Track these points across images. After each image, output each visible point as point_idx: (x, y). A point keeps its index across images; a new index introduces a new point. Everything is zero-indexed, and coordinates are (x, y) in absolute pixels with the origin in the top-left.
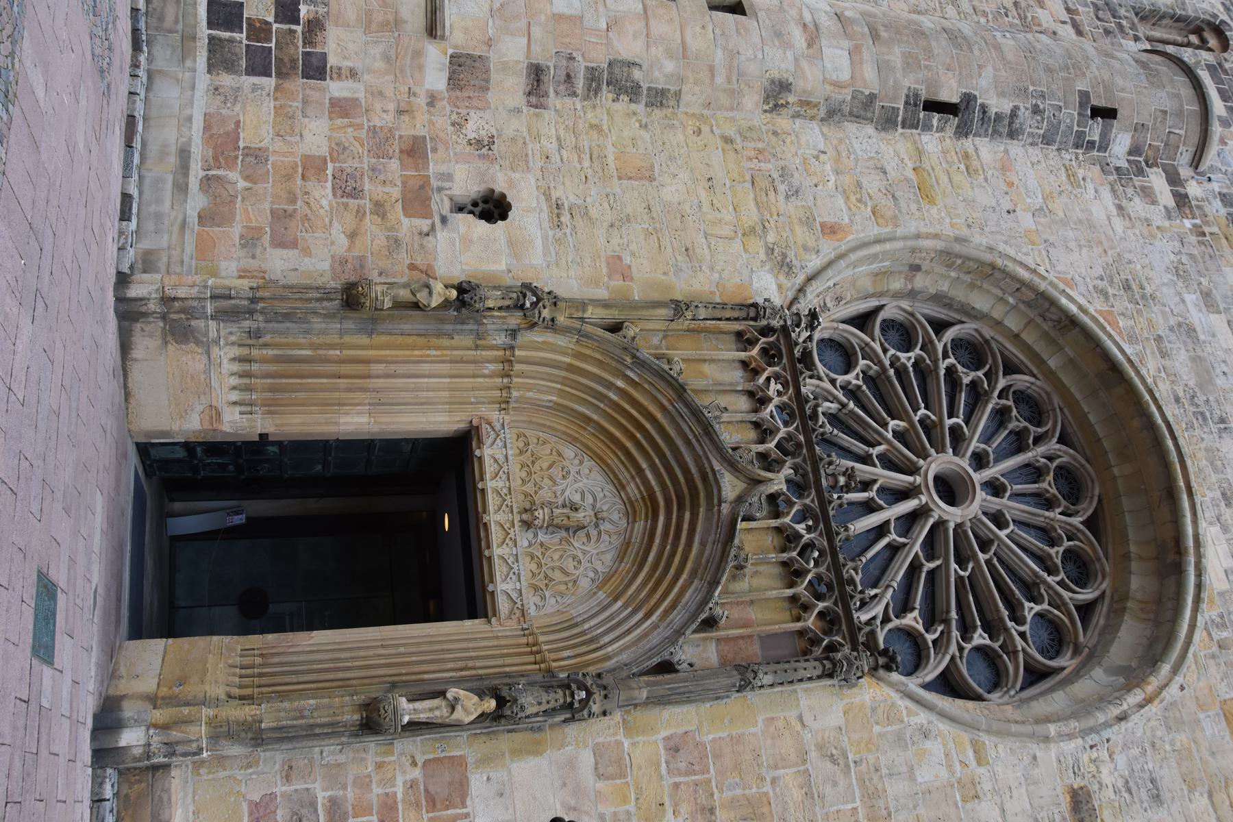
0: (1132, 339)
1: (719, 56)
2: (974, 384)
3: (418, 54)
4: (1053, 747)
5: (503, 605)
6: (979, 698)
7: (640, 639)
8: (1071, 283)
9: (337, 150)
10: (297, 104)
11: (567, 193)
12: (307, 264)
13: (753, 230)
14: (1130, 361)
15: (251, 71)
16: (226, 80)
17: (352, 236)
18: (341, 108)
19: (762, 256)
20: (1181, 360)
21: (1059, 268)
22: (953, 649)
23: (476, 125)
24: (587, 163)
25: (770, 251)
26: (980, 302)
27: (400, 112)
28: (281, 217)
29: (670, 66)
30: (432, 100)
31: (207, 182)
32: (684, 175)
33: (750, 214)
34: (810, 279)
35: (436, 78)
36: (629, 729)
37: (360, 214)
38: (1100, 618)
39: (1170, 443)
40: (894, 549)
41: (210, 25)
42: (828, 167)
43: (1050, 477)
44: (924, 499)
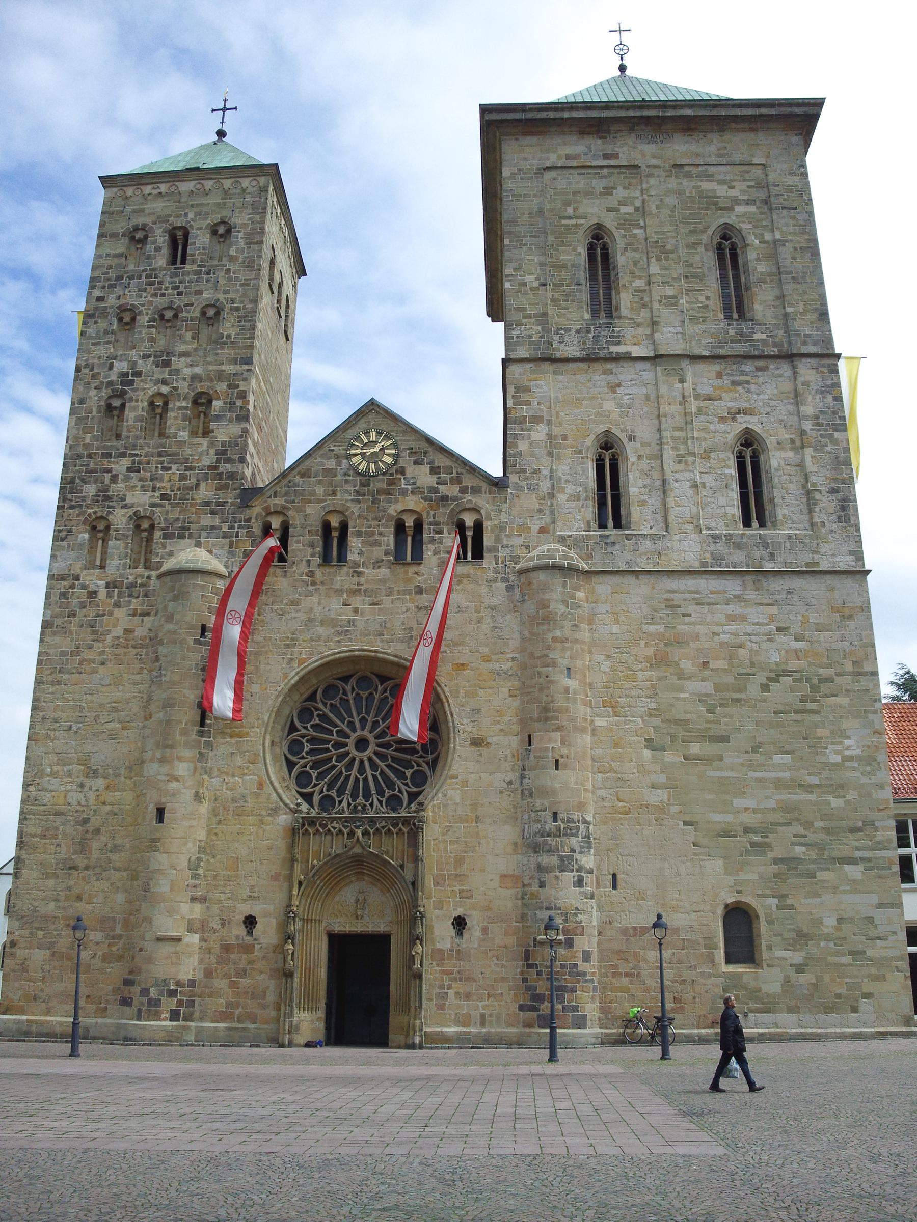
0: (312, 654)
1: (185, 823)
2: (319, 715)
3: (187, 945)
4: (458, 748)
5: (387, 929)
6: (439, 754)
8: (285, 676)
9: (226, 976)
10: (207, 990)
11: (246, 892)
12: (272, 988)
14: (322, 658)
15: (193, 1006)
16: (197, 1015)
17: (261, 972)
18: (208, 974)
19: (270, 818)
23: (215, 924)
24: (231, 883)
25: (269, 815)
26: (286, 711)
27: (210, 952)
29: (190, 845)
30: (202, 940)
31: (239, 1021)
32: (236, 845)
34: (281, 800)
35: (195, 938)
36: (429, 898)
37: (253, 969)
39: (357, 653)
40: (382, 773)
41: (178, 1021)
43: (361, 693)
44: (365, 758)
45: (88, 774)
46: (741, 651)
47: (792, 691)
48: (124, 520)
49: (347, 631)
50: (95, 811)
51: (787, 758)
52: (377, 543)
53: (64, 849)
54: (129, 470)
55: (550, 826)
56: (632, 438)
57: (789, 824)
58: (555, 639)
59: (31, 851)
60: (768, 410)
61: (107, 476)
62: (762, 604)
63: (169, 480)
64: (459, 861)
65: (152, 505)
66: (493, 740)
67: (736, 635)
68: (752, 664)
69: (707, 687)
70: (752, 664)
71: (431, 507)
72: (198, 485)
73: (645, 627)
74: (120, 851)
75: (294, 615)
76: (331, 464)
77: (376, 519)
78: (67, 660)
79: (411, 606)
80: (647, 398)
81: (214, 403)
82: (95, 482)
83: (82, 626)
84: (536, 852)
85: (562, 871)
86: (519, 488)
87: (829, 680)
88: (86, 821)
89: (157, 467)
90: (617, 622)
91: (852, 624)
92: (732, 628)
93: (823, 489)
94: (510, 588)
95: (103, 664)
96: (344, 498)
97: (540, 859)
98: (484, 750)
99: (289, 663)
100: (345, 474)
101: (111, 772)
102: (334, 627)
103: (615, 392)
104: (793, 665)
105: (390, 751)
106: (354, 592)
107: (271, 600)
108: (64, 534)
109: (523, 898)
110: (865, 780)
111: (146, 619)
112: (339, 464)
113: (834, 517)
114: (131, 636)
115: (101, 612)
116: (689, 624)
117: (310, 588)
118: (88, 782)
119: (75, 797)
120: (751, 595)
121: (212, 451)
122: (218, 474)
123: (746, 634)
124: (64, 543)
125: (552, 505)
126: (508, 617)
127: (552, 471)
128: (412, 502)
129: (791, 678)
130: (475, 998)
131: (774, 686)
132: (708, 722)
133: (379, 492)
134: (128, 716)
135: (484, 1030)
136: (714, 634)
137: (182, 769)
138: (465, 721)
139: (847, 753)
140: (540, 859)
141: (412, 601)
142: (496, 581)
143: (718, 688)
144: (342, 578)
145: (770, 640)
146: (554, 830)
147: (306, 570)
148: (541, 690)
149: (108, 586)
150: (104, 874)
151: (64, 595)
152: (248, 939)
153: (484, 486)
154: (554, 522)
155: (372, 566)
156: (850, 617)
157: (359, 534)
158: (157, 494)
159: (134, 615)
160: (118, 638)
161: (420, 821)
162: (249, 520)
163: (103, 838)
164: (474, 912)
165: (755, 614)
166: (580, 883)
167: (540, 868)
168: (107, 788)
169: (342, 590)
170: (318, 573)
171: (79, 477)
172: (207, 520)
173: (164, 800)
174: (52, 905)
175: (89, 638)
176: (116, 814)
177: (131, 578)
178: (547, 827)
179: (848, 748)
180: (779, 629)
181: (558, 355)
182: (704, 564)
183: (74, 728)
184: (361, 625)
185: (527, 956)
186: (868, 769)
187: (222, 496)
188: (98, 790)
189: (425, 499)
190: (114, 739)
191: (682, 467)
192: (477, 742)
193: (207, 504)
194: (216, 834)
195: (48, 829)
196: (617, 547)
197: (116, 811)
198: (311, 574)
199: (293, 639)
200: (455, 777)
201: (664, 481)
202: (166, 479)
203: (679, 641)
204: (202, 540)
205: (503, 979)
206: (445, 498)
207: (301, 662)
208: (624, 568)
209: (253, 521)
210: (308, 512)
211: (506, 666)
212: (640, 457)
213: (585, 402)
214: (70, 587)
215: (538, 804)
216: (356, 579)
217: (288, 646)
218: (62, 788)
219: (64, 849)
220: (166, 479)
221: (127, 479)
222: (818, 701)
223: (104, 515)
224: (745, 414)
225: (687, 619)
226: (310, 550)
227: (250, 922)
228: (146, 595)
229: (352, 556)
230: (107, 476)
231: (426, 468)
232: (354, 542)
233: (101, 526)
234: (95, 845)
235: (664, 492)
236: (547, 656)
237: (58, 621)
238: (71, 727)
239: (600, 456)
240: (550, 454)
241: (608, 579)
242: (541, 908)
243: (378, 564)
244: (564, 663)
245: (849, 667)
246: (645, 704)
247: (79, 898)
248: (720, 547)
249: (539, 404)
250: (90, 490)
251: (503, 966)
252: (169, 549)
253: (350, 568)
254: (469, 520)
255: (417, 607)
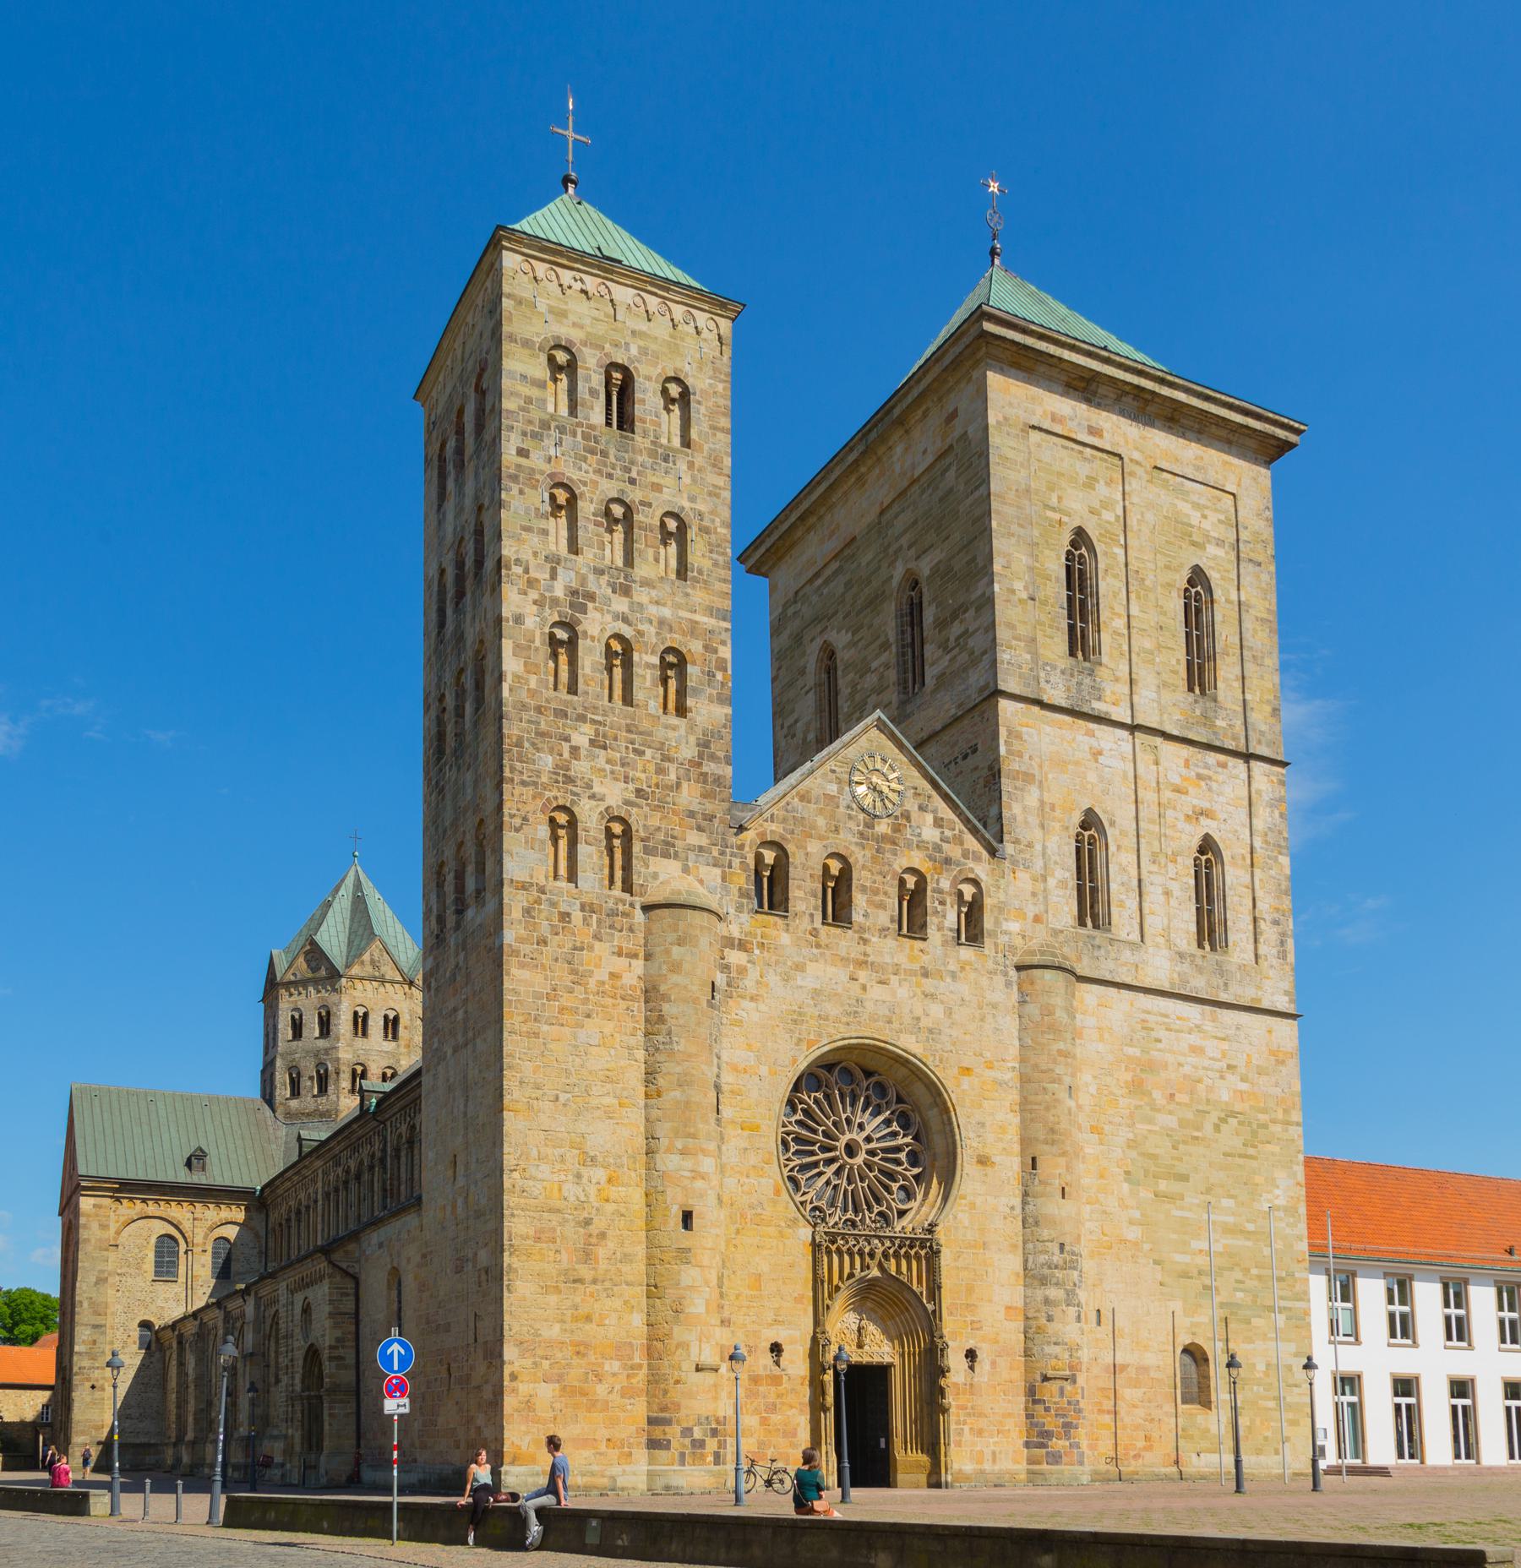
0: (820, 1035)
5: (891, 1360)
7: (918, 1318)
8: (794, 1061)
9: (756, 1411)
11: (770, 1316)
13: (780, 1232)
17: (791, 1407)
20: (833, 1010)
21: (787, 1063)
22: (908, 1173)
28: (785, 1434)
33: (771, 1230)
37: (783, 1404)
38: (903, 1093)
39: (867, 1041)
42: (747, 1181)
45: (585, 1161)
46: (1201, 1087)
47: (1237, 1134)
48: (595, 816)
49: (856, 1012)
50: (597, 1209)
51: (1230, 1203)
52: (881, 906)
53: (564, 1256)
54: (592, 742)
55: (1057, 1258)
56: (1112, 824)
57: (1231, 1269)
58: (1060, 1052)
59: (525, 1258)
60: (1225, 816)
61: (566, 746)
62: (1216, 1038)
63: (643, 773)
64: (970, 1290)
65: (627, 803)
66: (996, 1159)
67: (1194, 1067)
68: (1208, 1100)
69: (1171, 1121)
70: (1208, 1100)
71: (935, 869)
72: (678, 785)
73: (1125, 1048)
74: (631, 1261)
75: (799, 983)
76: (833, 789)
77: (880, 873)
78: (544, 1004)
79: (919, 991)
80: (1125, 773)
81: (690, 669)
82: (551, 751)
83: (556, 960)
84: (1043, 1284)
85: (1068, 1305)
86: (1015, 863)
87: (1265, 1126)
88: (587, 1222)
89: (627, 748)
90: (1102, 1039)
91: (1284, 1069)
92: (1192, 1059)
93: (1266, 916)
94: (1008, 984)
95: (588, 1016)
96: (847, 841)
97: (1048, 1292)
98: (989, 1170)
99: (797, 1044)
100: (848, 807)
101: (612, 1161)
102: (842, 1005)
103: (1096, 761)
104: (1238, 1107)
105: (876, 1159)
106: (861, 964)
107: (774, 958)
108: (517, 822)
109: (1025, 1332)
110: (1288, 1231)
111: (634, 962)
112: (840, 791)
113: (1274, 951)
114: (619, 984)
115: (578, 944)
116: (1159, 1050)
117: (815, 951)
118: (584, 1171)
119: (571, 1190)
120: (1208, 1026)
121: (692, 739)
122: (702, 774)
123: (1204, 1068)
124: (521, 836)
125: (1045, 890)
126: (1008, 1018)
127: (1044, 848)
128: (917, 860)
129: (1235, 1120)
130: (986, 1434)
131: (1224, 1127)
132: (1172, 1158)
133: (884, 838)
134: (624, 1089)
135: (997, 1468)
136: (1180, 1065)
137: (708, 1164)
138: (971, 1135)
139: (1277, 1202)
140: (1048, 1292)
141: (918, 985)
142: (996, 973)
143: (1182, 1123)
144: (842, 941)
145: (1222, 1077)
146: (1061, 1263)
147: (809, 928)
148: (1047, 1109)
149: (582, 909)
150: (615, 1288)
151: (527, 912)
152: (776, 1371)
153: (985, 854)
154: (1047, 912)
155: (877, 934)
156: (1283, 1062)
157: (864, 889)
158: (631, 787)
159: (620, 954)
160: (603, 983)
161: (938, 1244)
162: (741, 847)
163: (611, 1244)
164: (984, 1346)
165: (1212, 1048)
166: (1079, 1319)
167: (1047, 1301)
168: (610, 1181)
169: (848, 959)
170: (824, 930)
171: (528, 740)
172: (695, 838)
173: (690, 1202)
174: (557, 1327)
175: (568, 979)
176: (622, 1215)
177: (611, 904)
178: (1055, 1259)
179: (1277, 1197)
180: (1229, 1067)
181: (1045, 699)
182: (1172, 984)
183: (563, 1097)
184: (869, 1005)
185: (1031, 1391)
186: (1292, 1220)
187: (709, 807)
188: (598, 1183)
189: (930, 858)
190: (610, 1118)
191: (1154, 868)
192: (983, 1161)
193: (692, 814)
194: (735, 1246)
195: (542, 1231)
196: (1102, 952)
197: (623, 1211)
198: (814, 933)
199: (800, 1014)
200: (964, 1197)
201: (1140, 881)
202: (640, 767)
203: (1150, 1067)
204: (690, 864)
205: (1010, 1415)
206: (948, 861)
207: (810, 1044)
208: (1108, 977)
209: (747, 848)
210: (809, 849)
211: (1008, 1076)
212: (1119, 847)
213: (1070, 767)
214: (535, 902)
215: (1046, 1233)
216: (861, 948)
217: (795, 1021)
218: (555, 1178)
219: (564, 1256)
220: (640, 767)
221: (591, 757)
222: (1255, 1147)
223: (568, 805)
224: (1207, 816)
225: (1159, 1045)
226: (813, 901)
227: (776, 1349)
228: (631, 930)
229: (857, 917)
230: (566, 746)
231: (929, 818)
232: (859, 900)
233: (562, 818)
234: (601, 1252)
235: (1140, 896)
236: (1052, 1070)
237: (526, 948)
238: (557, 1099)
239: (1077, 835)
240: (1042, 826)
241: (1094, 987)
242: (1049, 1343)
243: (883, 931)
244: (1067, 1080)
245: (1280, 1116)
246: (1125, 1134)
247: (588, 1319)
248: (1186, 967)
249: (1031, 758)
250: (547, 761)
251: (1009, 1401)
252: (652, 869)
253: (855, 932)
254: (968, 891)
255: (923, 993)
